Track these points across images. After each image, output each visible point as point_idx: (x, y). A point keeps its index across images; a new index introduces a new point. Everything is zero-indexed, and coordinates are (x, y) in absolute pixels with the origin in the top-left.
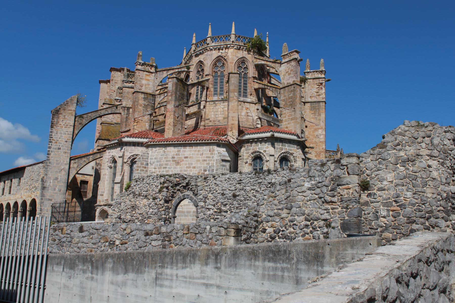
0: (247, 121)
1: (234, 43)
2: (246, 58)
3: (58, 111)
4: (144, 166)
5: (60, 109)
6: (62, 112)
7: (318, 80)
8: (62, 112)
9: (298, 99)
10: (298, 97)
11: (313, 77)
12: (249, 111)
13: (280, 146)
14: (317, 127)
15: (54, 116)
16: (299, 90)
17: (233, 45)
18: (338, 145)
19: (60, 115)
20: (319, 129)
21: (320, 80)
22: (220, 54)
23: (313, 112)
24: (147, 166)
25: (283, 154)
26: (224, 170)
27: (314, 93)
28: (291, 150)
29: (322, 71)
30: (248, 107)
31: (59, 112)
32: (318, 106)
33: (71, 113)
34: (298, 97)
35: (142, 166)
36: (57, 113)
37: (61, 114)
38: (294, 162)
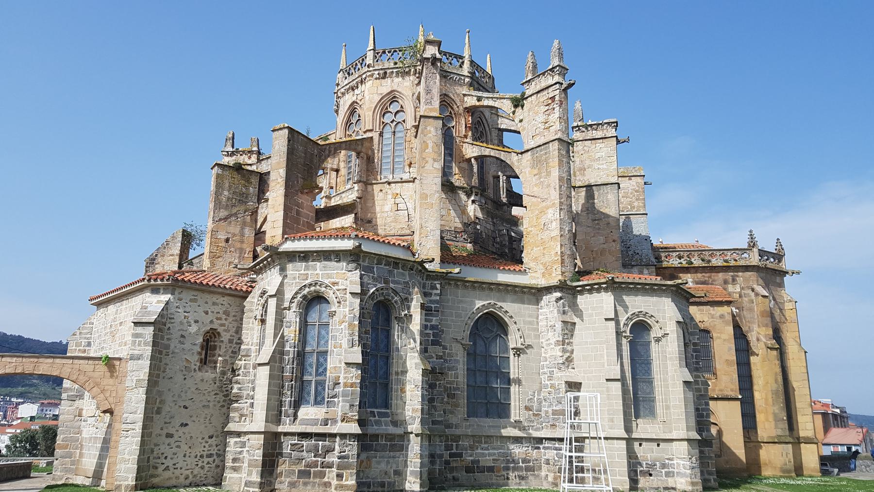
0: (396, 221)
1: (371, 69)
2: (398, 92)
3: (154, 259)
4: (81, 348)
5: (156, 255)
6: (159, 261)
7: (545, 92)
8: (159, 261)
11: (538, 88)
12: (398, 200)
13: (302, 272)
14: (544, 204)
15: (148, 269)
16: (432, 129)
17: (370, 73)
18: (751, 231)
19: (156, 266)
20: (548, 208)
21: (551, 89)
22: (354, 99)
23: (536, 171)
24: (87, 348)
25: (307, 290)
26: (139, 345)
27: (540, 125)
28: (329, 276)
29: (552, 70)
30: (398, 192)
31: (156, 262)
32: (546, 153)
33: (173, 259)
35: (78, 348)
36: (153, 263)
37: (158, 263)
38: (337, 305)
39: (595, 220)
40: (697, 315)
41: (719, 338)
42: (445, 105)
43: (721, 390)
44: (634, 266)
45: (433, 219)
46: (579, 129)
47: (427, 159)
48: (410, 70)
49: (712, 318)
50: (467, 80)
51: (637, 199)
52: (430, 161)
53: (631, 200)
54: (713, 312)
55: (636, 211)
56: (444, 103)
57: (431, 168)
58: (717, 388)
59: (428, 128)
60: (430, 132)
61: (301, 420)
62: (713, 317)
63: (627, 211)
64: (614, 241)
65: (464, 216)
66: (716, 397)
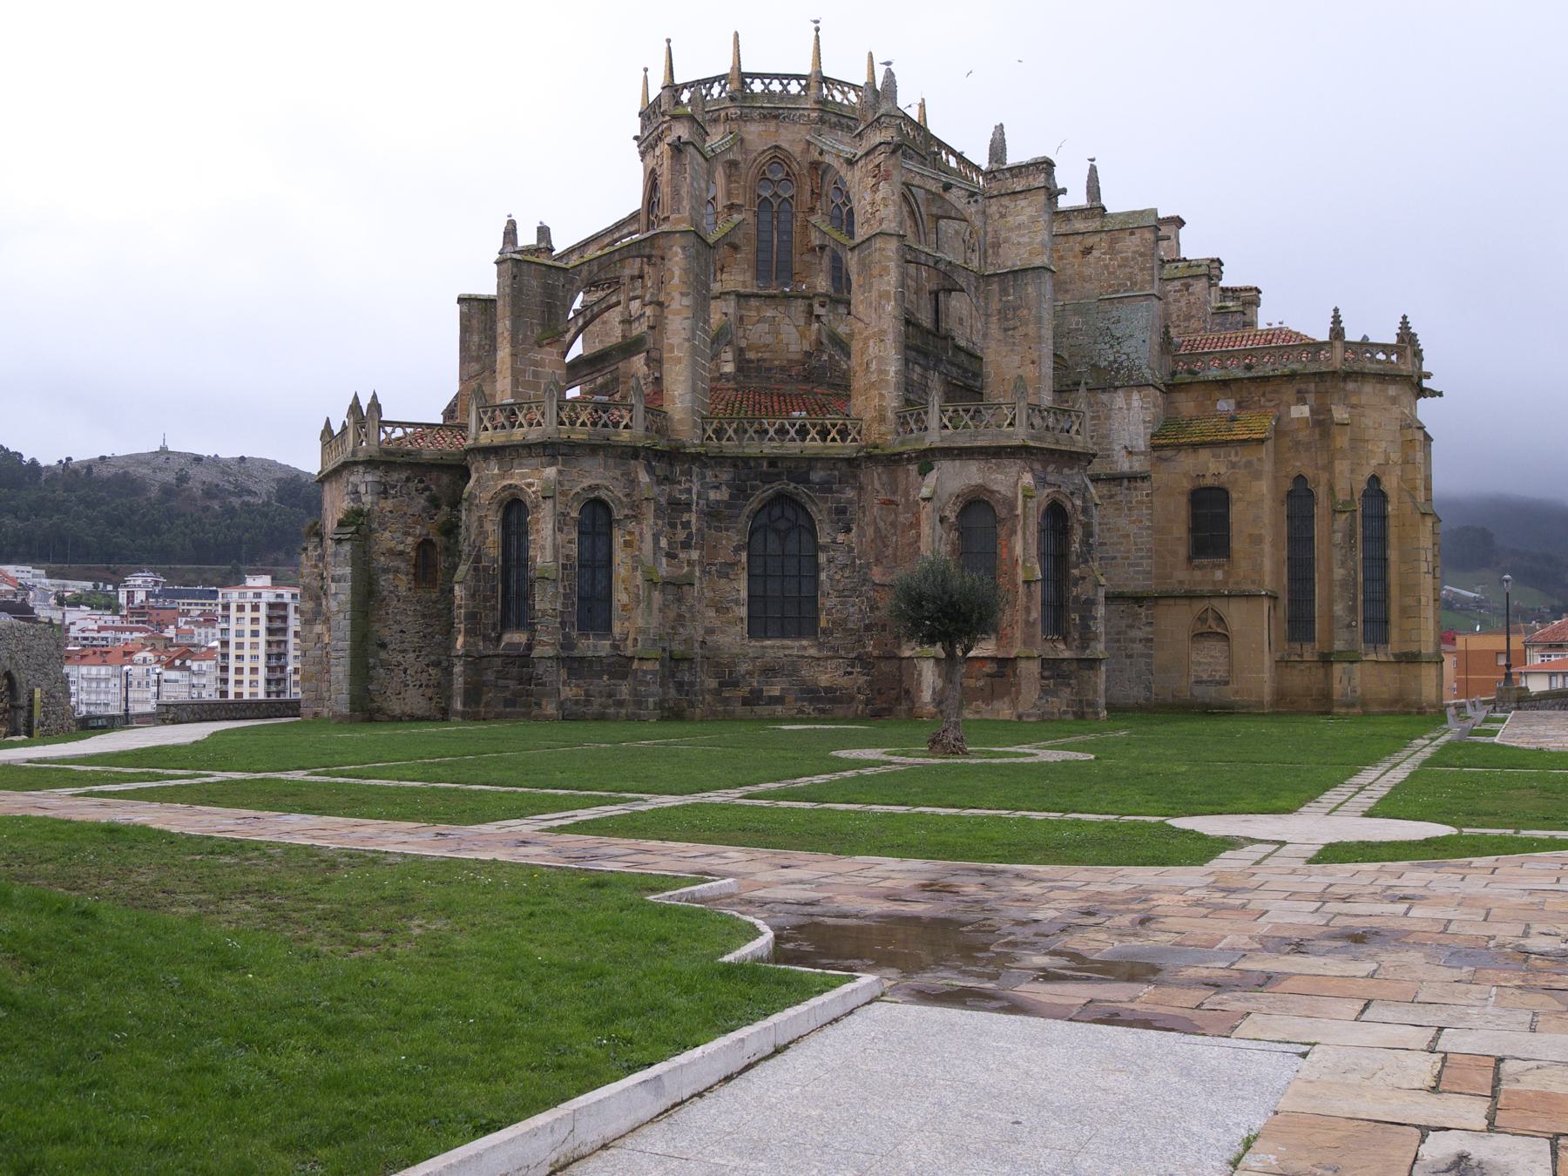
3: (453, 411)
9: (676, 280)
10: (677, 272)
16: (679, 250)
17: (665, 125)
34: (677, 272)
39: (1009, 329)
40: (1210, 465)
41: (1240, 499)
42: (779, 163)
43: (1237, 583)
44: (1116, 388)
45: (682, 378)
46: (995, 176)
47: (673, 294)
48: (719, 116)
49: (1233, 468)
50: (814, 115)
51: (1141, 270)
52: (676, 295)
53: (1130, 270)
54: (1234, 459)
55: (1140, 290)
56: (776, 160)
57: (679, 307)
58: (1231, 580)
59: (674, 248)
60: (676, 253)
61: (508, 644)
62: (1234, 465)
63: (1125, 291)
64: (1033, 362)
65: (804, 341)
66: (1226, 593)
